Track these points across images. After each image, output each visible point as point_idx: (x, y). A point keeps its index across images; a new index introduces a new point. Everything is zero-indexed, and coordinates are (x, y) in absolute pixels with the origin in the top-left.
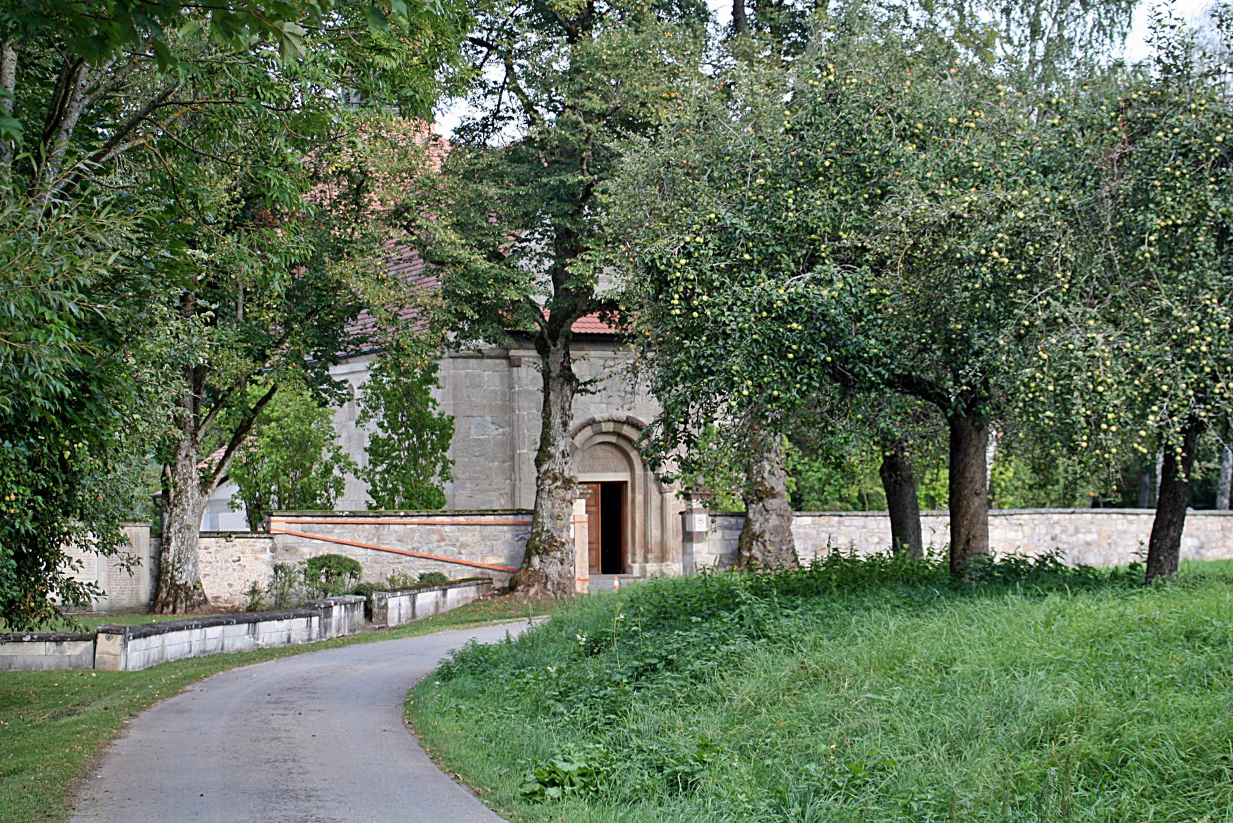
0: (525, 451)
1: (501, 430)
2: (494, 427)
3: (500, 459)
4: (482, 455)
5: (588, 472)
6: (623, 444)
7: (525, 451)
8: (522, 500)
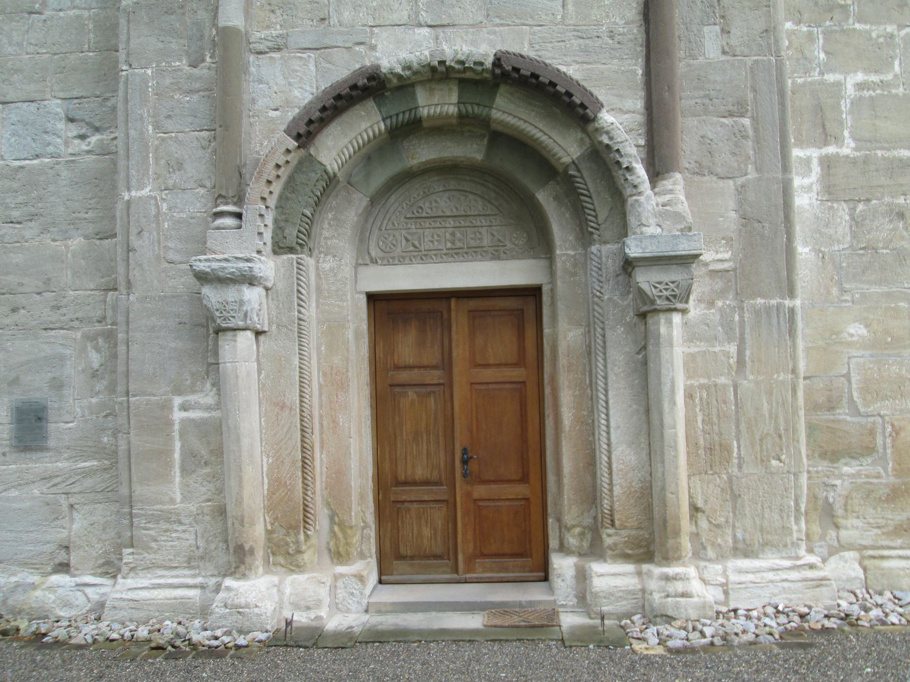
0: (146, 192)
1: (94, 139)
2: (74, 130)
3: (90, 229)
4: (32, 217)
5: (402, 260)
6: (508, 165)
7: (146, 192)
8: (134, 348)
